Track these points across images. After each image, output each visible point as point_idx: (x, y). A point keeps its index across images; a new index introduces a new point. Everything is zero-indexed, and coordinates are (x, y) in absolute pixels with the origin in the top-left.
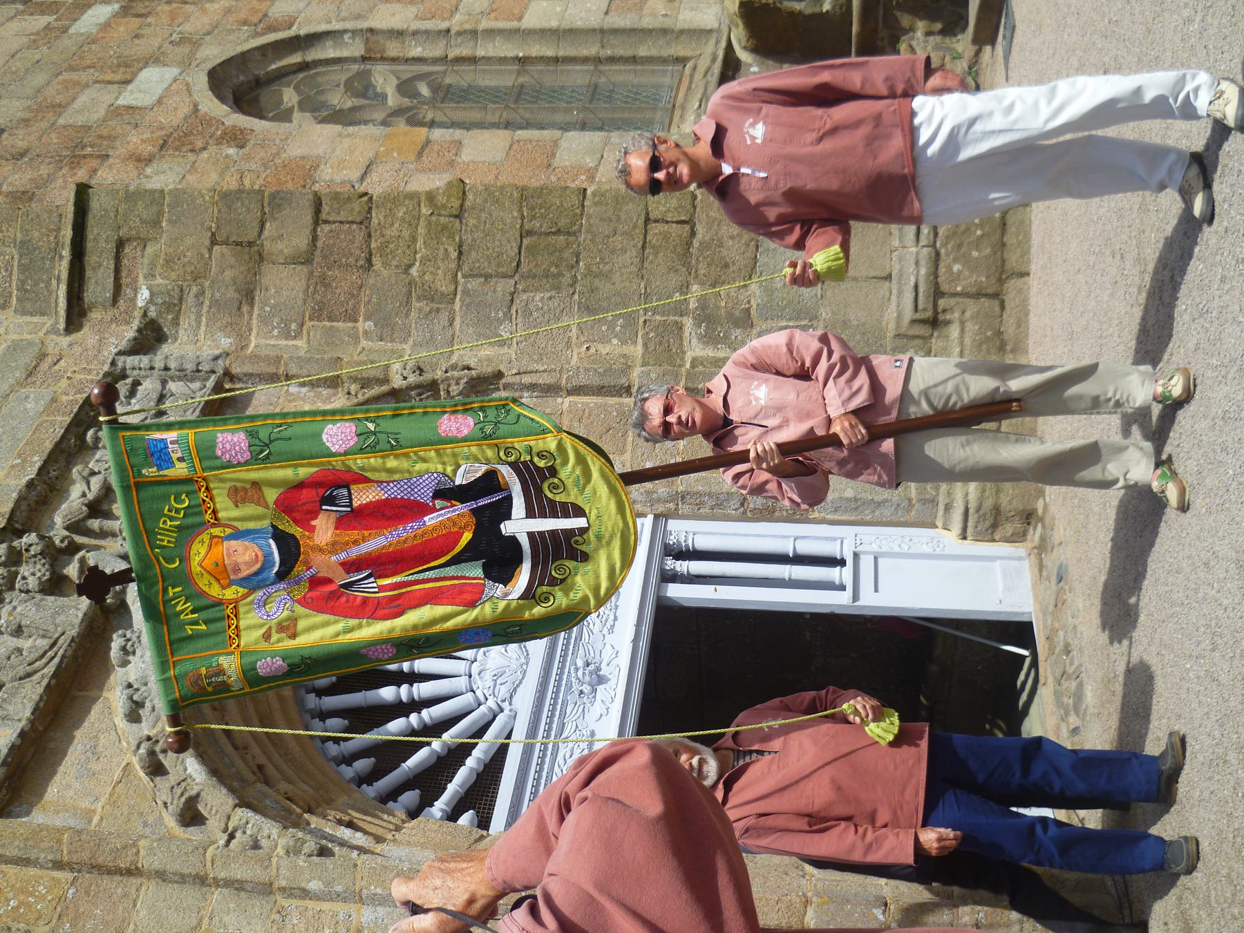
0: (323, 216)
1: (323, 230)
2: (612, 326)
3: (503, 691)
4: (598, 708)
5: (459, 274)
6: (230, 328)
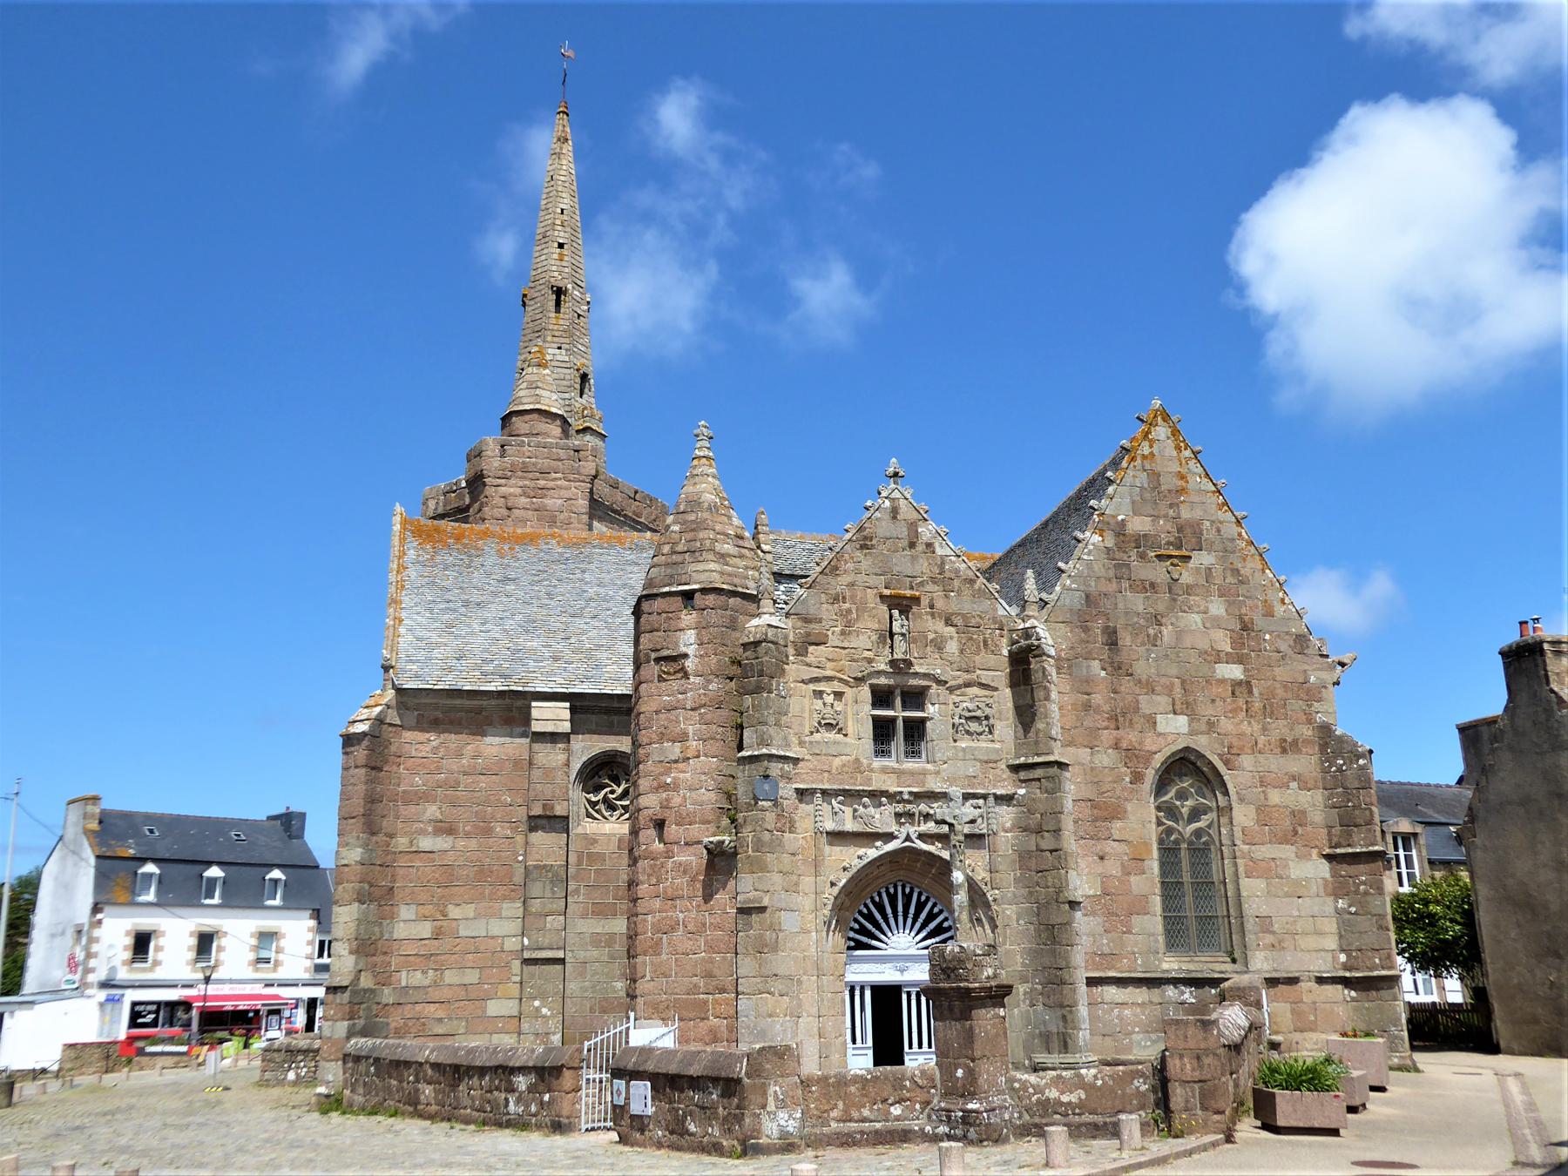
1: (1048, 854)
3: (893, 945)
4: (892, 972)
6: (1013, 826)
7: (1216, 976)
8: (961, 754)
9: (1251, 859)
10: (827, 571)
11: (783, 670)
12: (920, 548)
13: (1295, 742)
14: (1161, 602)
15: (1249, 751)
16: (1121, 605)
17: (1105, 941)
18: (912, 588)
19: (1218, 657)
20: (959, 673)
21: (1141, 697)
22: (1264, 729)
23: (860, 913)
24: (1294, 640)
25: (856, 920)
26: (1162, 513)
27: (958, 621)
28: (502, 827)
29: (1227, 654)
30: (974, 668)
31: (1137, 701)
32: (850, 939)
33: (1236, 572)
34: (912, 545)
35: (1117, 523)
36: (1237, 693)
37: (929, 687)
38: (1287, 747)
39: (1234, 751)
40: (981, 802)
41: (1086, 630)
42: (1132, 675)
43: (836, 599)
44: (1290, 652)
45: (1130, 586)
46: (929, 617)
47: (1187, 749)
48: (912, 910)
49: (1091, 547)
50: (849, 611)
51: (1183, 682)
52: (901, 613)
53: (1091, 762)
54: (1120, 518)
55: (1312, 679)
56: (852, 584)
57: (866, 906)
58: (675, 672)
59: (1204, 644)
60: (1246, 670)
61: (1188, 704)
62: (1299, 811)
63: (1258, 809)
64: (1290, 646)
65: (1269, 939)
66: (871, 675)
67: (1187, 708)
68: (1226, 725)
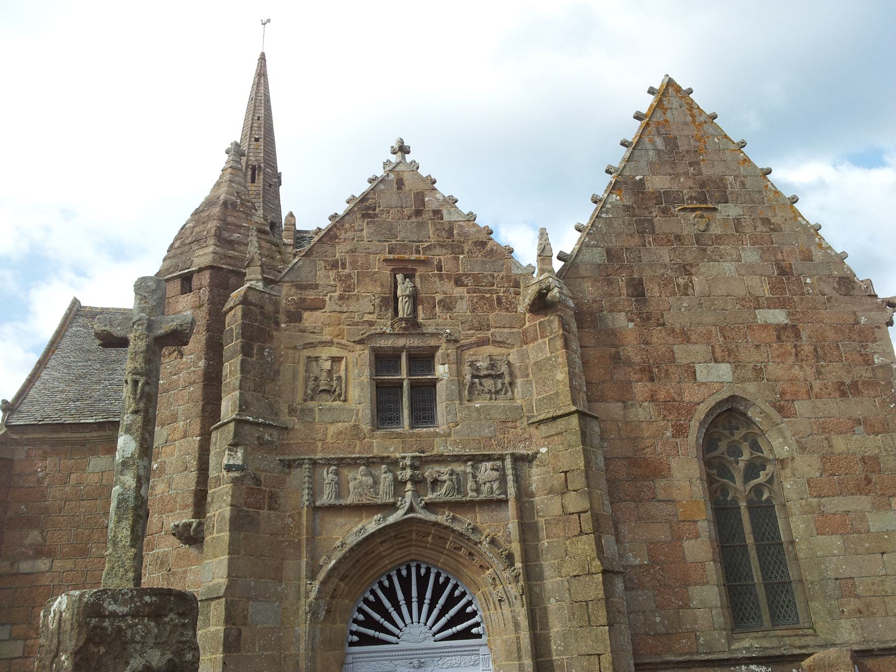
0: (582, 515)
2: (560, 645)
5: (568, 577)
7: (797, 651)
8: (474, 414)
9: (822, 514)
10: (324, 240)
11: (271, 337)
12: (427, 216)
13: (854, 384)
14: (691, 254)
15: (805, 396)
16: (645, 259)
17: (658, 620)
18: (418, 252)
19: (757, 303)
20: (472, 332)
21: (675, 347)
22: (819, 373)
23: (366, 601)
24: (839, 284)
25: (360, 610)
26: (681, 171)
27: (469, 281)
28: (97, 548)
29: (767, 299)
30: (488, 325)
31: (672, 351)
32: (352, 633)
33: (766, 221)
34: (418, 213)
35: (636, 182)
36: (783, 338)
37: (437, 348)
38: (844, 390)
39: (788, 397)
40: (499, 463)
41: (610, 283)
42: (663, 325)
43: (334, 265)
44: (835, 294)
45: (654, 240)
46: (437, 279)
47: (733, 398)
48: (428, 595)
49: (609, 206)
50: (349, 276)
51: (722, 330)
52: (406, 277)
53: (625, 416)
54: (638, 178)
55: (863, 320)
56: (353, 251)
57: (373, 592)
58: (170, 354)
59: (740, 291)
60: (789, 314)
61: (730, 352)
62: (870, 458)
63: (823, 458)
64: (834, 288)
65: (854, 604)
66: (371, 337)
67: (729, 355)
68: (774, 370)
